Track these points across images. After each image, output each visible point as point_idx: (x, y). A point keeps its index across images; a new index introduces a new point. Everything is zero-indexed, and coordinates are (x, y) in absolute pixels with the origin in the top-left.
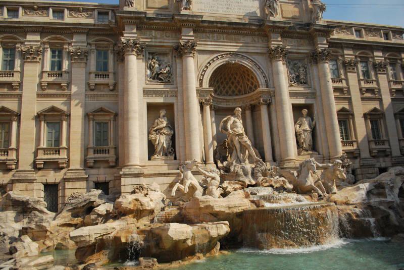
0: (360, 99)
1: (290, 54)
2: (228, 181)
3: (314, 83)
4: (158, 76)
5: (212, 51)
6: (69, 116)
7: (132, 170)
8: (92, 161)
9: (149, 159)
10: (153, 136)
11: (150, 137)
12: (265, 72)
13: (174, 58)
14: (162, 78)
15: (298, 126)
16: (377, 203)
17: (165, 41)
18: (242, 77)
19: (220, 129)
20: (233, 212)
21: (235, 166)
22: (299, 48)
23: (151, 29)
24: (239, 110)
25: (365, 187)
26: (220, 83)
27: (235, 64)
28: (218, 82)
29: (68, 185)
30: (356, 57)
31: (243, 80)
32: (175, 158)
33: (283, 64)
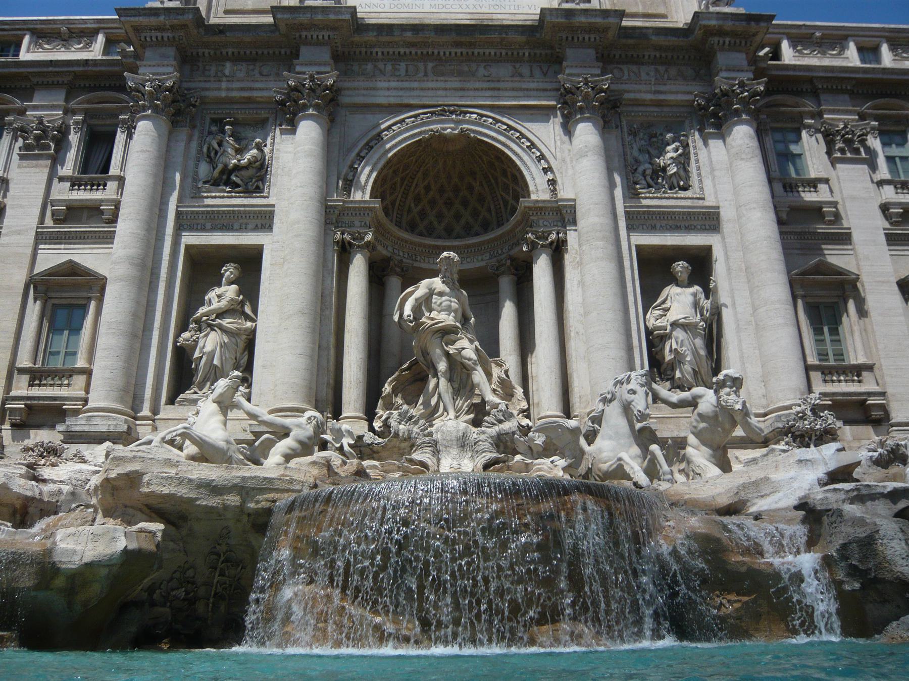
0: (883, 238)
1: (636, 109)
4: (229, 178)
11: (181, 339)
17: (258, 85)
20: (226, 507)
22: (662, 88)
28: (417, 199)
30: (862, 117)
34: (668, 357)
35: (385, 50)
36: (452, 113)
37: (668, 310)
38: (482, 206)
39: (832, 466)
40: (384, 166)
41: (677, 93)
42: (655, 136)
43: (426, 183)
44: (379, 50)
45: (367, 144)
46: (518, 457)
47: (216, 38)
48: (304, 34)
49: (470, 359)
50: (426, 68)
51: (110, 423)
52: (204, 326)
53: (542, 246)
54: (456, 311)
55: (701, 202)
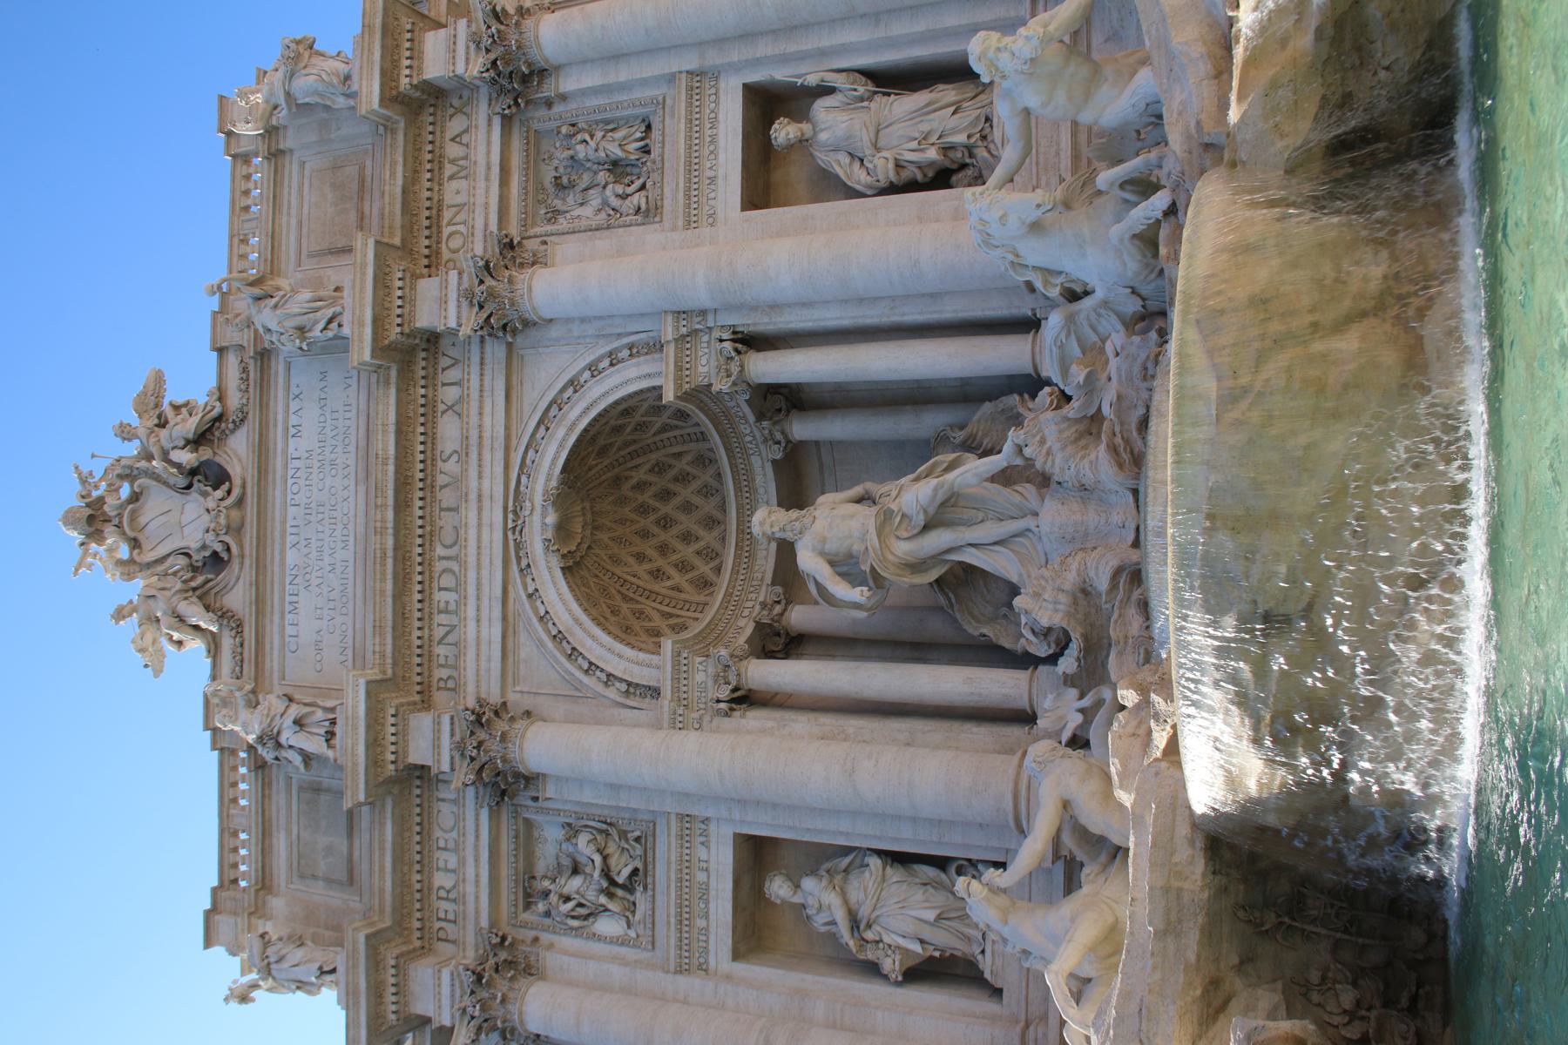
3: (644, 82)
4: (623, 887)
5: (505, 618)
9: (997, 993)
10: (891, 965)
12: (592, 357)
13: (540, 803)
14: (626, 872)
18: (634, 455)
19: (862, 615)
22: (481, 170)
23: (426, 890)
24: (762, 524)
26: (660, 562)
28: (657, 574)
31: (647, 450)
34: (932, 154)
35: (418, 624)
41: (489, 143)
43: (632, 561)
46: (1106, 410)
49: (936, 490)
50: (441, 558)
52: (869, 935)
55: (668, 102)
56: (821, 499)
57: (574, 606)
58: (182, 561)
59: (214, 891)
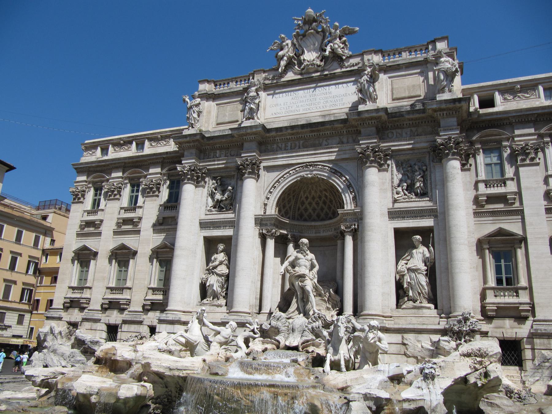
0: (544, 210)
1: (400, 153)
2: (262, 339)
6: (135, 253)
7: (168, 315)
8: (149, 303)
14: (222, 206)
15: (406, 262)
16: (361, 396)
18: (333, 196)
21: (278, 319)
25: (387, 369)
26: (307, 203)
27: (312, 178)
29: (125, 327)
31: (334, 198)
32: (226, 305)
33: (379, 171)
34: (405, 286)
36: (310, 166)
37: (408, 260)
38: (332, 204)
39: (391, 374)
40: (281, 195)
41: (421, 143)
42: (411, 166)
43: (305, 196)
44: (278, 138)
45: (273, 185)
47: (211, 142)
48: (244, 137)
50: (299, 144)
51: (174, 316)
53: (348, 232)
54: (306, 266)
56: (313, 255)
57: (287, 185)
58: (300, 52)
59: (213, 81)
